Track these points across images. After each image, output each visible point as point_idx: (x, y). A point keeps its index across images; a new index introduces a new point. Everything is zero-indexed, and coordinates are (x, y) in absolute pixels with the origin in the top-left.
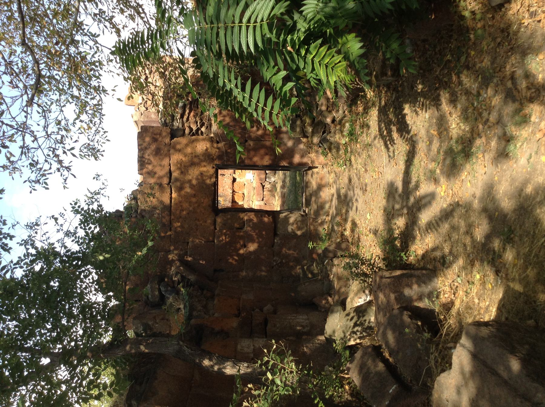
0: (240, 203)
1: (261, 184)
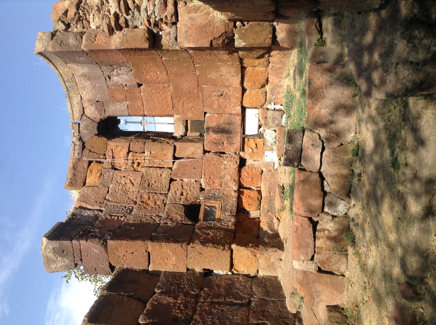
0: (254, 214)
1: (310, 219)
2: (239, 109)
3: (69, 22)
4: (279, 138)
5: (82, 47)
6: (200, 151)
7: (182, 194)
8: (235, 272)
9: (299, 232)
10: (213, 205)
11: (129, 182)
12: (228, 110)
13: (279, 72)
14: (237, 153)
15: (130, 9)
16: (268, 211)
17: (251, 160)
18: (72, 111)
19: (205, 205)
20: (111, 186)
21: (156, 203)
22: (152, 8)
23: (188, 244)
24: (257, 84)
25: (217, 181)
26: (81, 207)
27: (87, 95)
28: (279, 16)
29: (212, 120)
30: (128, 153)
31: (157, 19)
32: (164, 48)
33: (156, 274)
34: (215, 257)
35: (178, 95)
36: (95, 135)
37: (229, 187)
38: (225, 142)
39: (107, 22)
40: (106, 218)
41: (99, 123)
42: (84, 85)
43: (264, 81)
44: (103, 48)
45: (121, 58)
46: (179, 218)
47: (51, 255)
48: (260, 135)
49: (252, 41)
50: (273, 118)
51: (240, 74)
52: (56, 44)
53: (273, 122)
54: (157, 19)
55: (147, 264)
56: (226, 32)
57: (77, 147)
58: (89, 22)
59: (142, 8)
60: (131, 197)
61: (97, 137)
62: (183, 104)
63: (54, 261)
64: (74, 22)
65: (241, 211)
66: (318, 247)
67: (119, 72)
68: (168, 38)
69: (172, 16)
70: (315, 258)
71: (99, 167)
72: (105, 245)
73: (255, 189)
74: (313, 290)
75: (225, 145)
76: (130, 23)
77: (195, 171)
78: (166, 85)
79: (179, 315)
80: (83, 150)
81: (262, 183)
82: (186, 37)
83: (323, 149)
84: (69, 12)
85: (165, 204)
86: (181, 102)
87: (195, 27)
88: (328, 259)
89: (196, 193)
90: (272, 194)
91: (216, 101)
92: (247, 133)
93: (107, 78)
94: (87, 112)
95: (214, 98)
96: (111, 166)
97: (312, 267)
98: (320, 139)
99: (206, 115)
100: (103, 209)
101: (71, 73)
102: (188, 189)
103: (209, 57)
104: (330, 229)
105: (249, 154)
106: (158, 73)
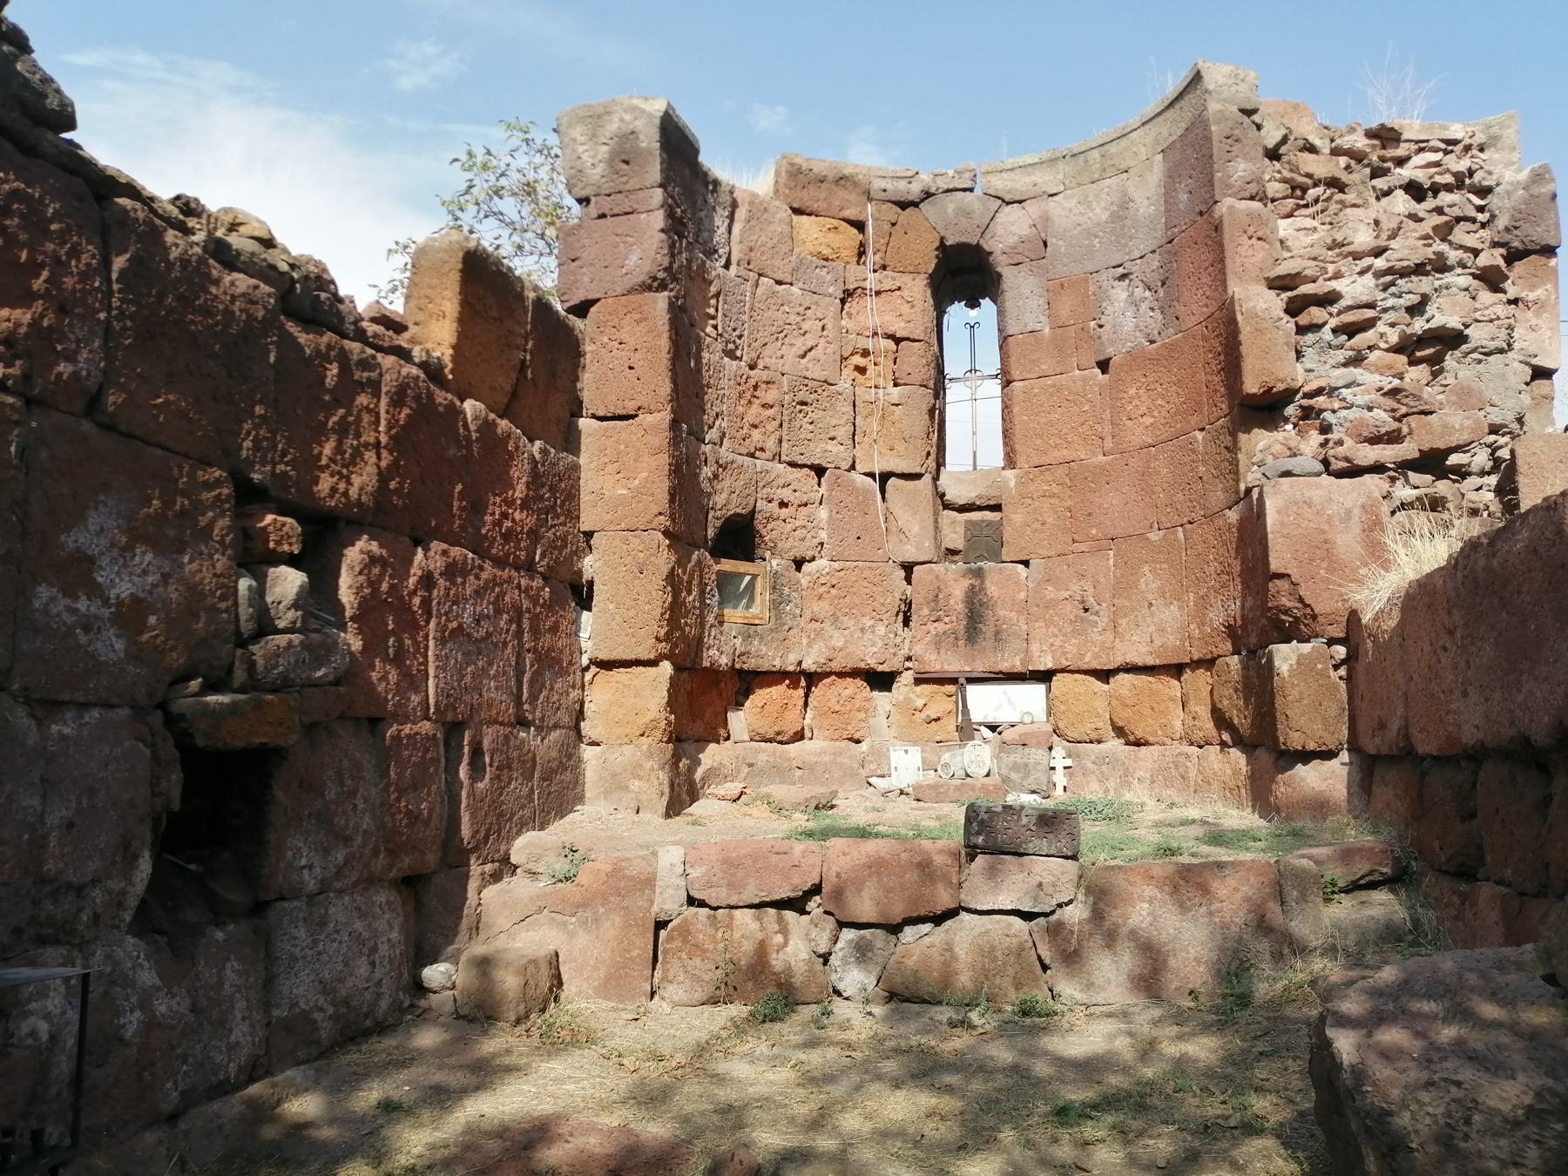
0: (739, 721)
1: (816, 890)
2: (1047, 663)
3: (1285, 159)
4: (973, 788)
5: (1228, 201)
6: (910, 554)
7: (783, 505)
8: (588, 676)
9: (775, 858)
10: (758, 599)
11: (809, 344)
12: (1039, 629)
13: (1163, 776)
14: (908, 664)
15: (1351, 337)
16: (751, 765)
17: (888, 707)
18: (1012, 170)
19: (755, 577)
20: (794, 289)
21: (755, 427)
22: (1360, 400)
23: (666, 533)
24: (1127, 713)
25: (822, 608)
26: (734, 205)
27: (1064, 211)
28: (1368, 768)
29: (1006, 584)
30: (892, 337)
31: (1327, 415)
32: (1242, 437)
33: (571, 441)
34: (632, 613)
35: (1078, 478)
36: (942, 239)
37: (809, 645)
38: (940, 627)
39: (1308, 272)
40: (711, 283)
41: (978, 248)
42: (1094, 204)
43: (1139, 734)
44: (1228, 262)
45: (1196, 309)
46: (720, 499)
47: (613, 126)
48: (966, 731)
49: (1293, 694)
50: (1026, 765)
51: (1158, 662)
52: (1230, 124)
53: (1015, 767)
54: (1327, 415)
55: (601, 413)
56: (1314, 617)
57: (902, 185)
58: (1290, 215)
59: (1356, 373)
60: (767, 351)
61: (937, 244)
62: (1053, 496)
63: (594, 135)
64: (1286, 174)
65: (746, 681)
66: (732, 918)
67: (1144, 306)
68: (1277, 448)
69: (1347, 459)
70: (693, 910)
71: (849, 253)
72: (654, 285)
73: (807, 722)
74: (602, 910)
75: (932, 627)
76: (1310, 338)
77: (852, 539)
78: (1109, 444)
79: (488, 518)
80: (894, 203)
81: (826, 743)
82: (1296, 503)
83: (1028, 916)
84: (1313, 156)
85: (752, 455)
86: (1056, 489)
87: (1326, 527)
88: (698, 950)
89: (788, 545)
90: (798, 773)
91: (1067, 594)
92: (973, 691)
93: (1121, 270)
94: (1010, 214)
95: (1076, 588)
96: (851, 287)
97: (668, 901)
98: (1060, 906)
99: (1021, 567)
100: (733, 269)
101: (1131, 163)
102: (798, 523)
103: (1213, 567)
104: (789, 949)
105: (908, 700)
106: (1148, 420)
